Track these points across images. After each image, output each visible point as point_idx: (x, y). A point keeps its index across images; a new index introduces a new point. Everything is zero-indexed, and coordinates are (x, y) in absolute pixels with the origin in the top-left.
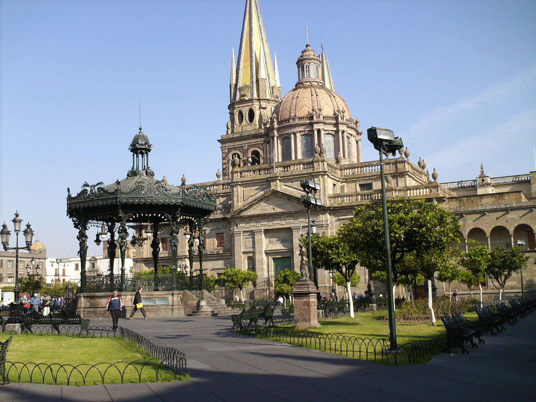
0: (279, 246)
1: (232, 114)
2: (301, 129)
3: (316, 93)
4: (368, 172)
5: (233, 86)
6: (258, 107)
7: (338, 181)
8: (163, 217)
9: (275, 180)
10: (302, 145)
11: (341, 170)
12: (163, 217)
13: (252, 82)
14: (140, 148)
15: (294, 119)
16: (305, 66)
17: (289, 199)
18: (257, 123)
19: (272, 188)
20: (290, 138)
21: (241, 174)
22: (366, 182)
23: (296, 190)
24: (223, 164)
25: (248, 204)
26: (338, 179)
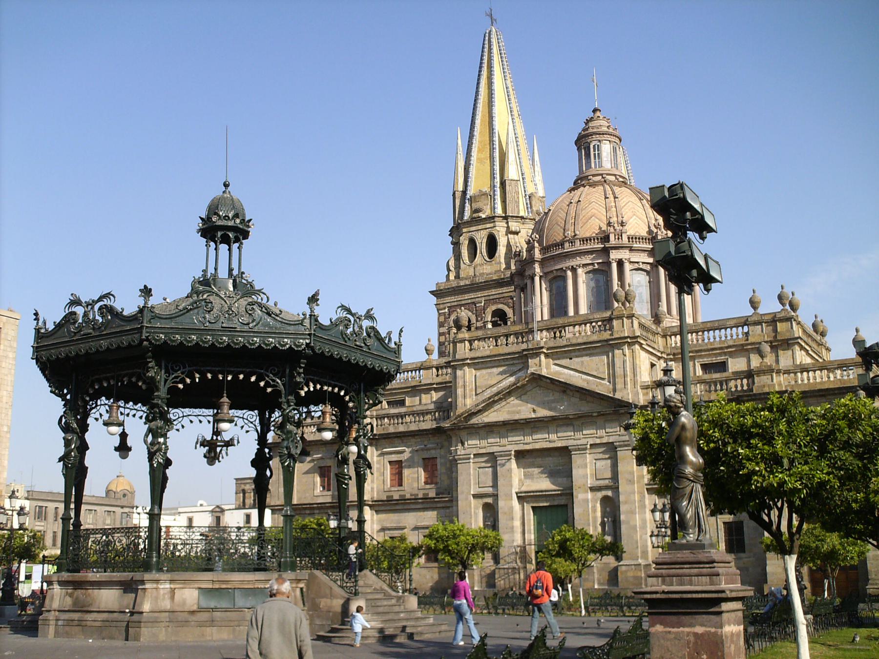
0: (544, 484)
1: (456, 245)
2: (587, 260)
3: (614, 193)
4: (718, 339)
5: (458, 195)
6: (503, 230)
7: (659, 358)
8: (262, 384)
9: (537, 355)
10: (587, 290)
11: (664, 336)
12: (262, 384)
13: (493, 187)
14: (223, 228)
15: (572, 242)
16: (592, 146)
17: (564, 392)
18: (502, 260)
19: (531, 370)
20: (564, 278)
21: (471, 345)
22: (714, 360)
23: (577, 374)
24: (440, 334)
25: (484, 401)
26: (659, 354)
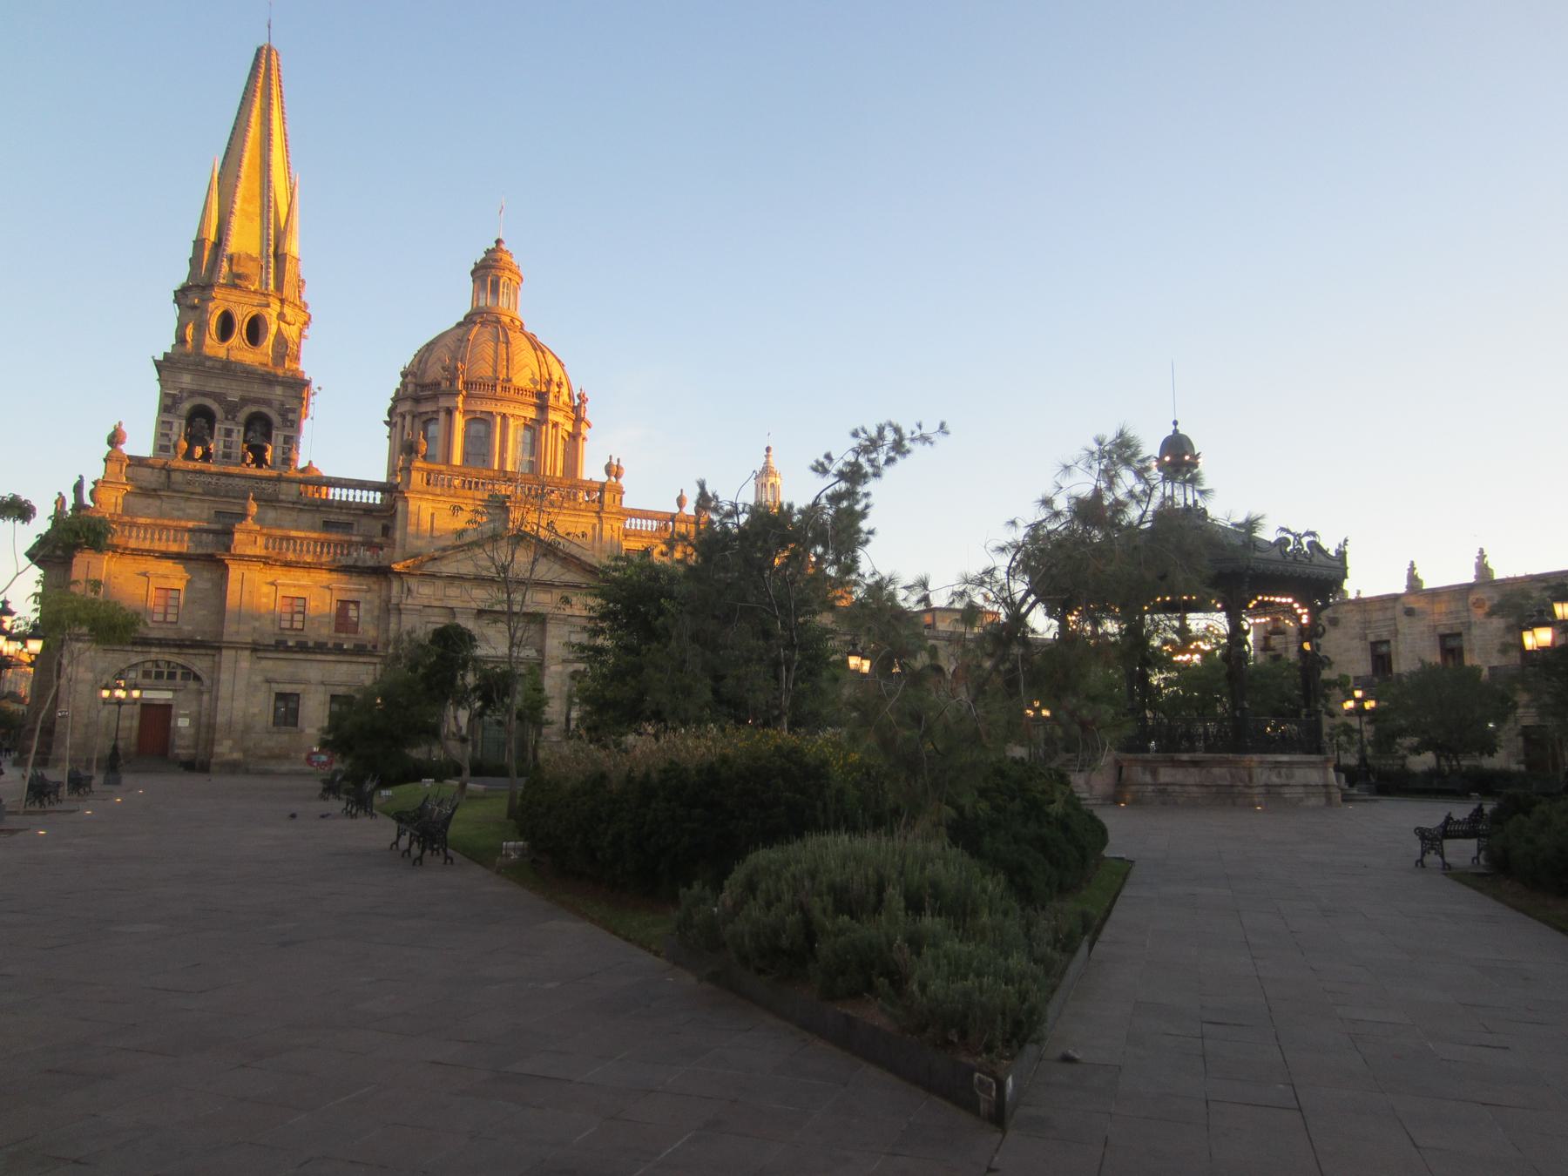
5: (208, 245)
6: (275, 314)
